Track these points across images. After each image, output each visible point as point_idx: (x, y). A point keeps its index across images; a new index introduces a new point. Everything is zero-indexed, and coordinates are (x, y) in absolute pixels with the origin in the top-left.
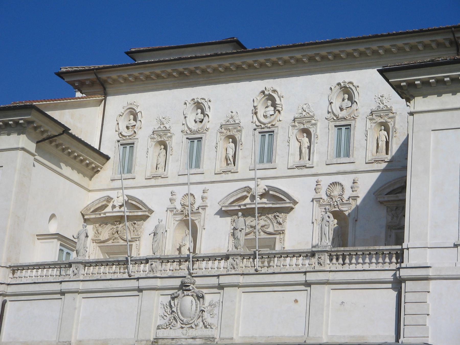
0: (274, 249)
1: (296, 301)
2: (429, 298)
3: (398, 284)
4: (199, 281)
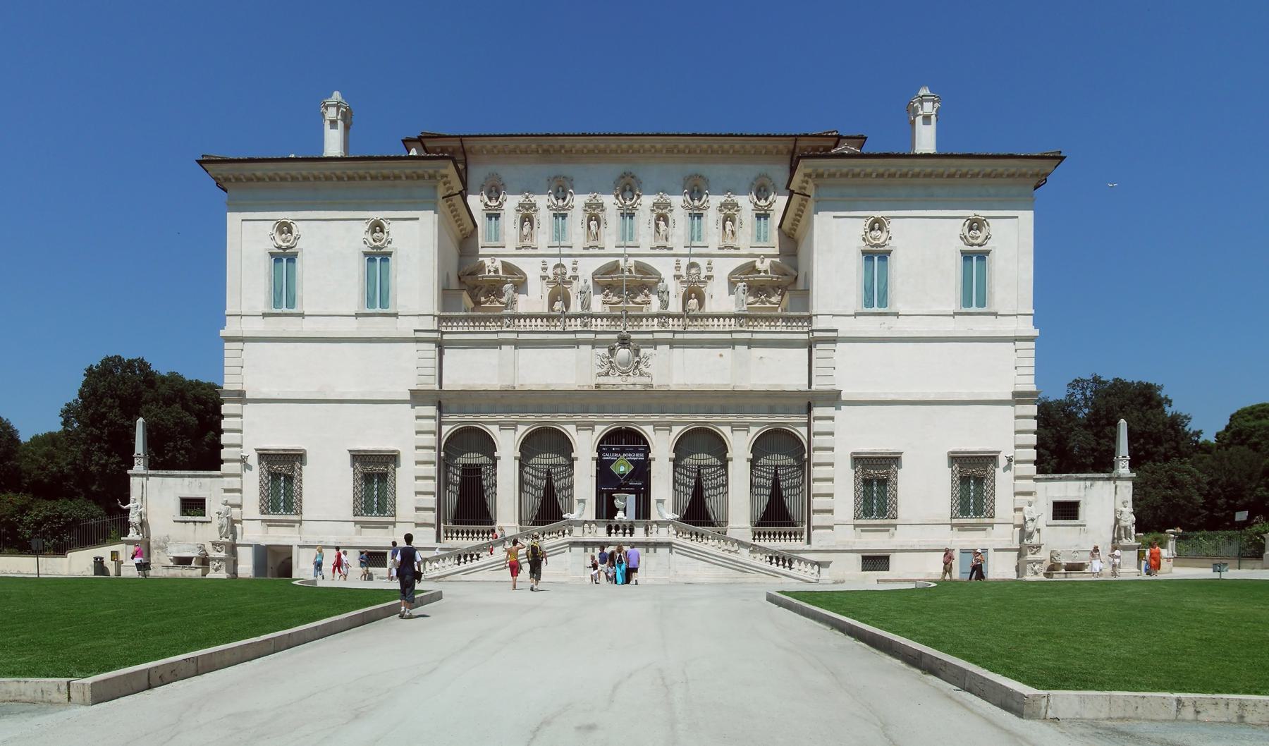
2: (835, 355)
4: (633, 337)
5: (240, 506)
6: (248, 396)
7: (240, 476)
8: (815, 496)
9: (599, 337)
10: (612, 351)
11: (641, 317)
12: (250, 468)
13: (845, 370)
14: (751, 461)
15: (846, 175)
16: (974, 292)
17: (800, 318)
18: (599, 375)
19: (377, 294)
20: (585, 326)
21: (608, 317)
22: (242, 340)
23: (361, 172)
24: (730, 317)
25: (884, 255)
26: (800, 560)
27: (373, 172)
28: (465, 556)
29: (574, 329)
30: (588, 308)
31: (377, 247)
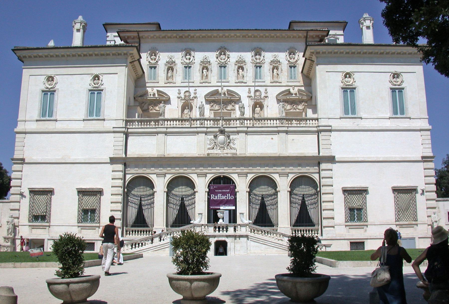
0: (231, 117)
1: (272, 139)
2: (331, 138)
5: (18, 218)
6: (26, 161)
7: (19, 202)
8: (323, 210)
9: (209, 130)
10: (216, 137)
11: (230, 120)
12: (25, 197)
13: (337, 145)
14: (290, 192)
15: (331, 53)
18: (209, 149)
19: (94, 109)
20: (202, 124)
21: (214, 120)
22: (25, 133)
23: (91, 53)
24: (276, 119)
25: (353, 90)
27: (96, 53)
29: (195, 126)
30: (203, 115)
31: (96, 87)
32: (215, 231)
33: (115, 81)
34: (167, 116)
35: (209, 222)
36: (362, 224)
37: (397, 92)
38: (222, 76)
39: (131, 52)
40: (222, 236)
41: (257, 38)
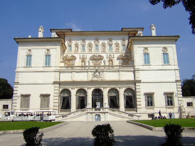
3: (134, 72)
4: (99, 70)
11: (100, 67)
16: (166, 60)
17: (132, 66)
20: (89, 68)
21: (94, 67)
26: (135, 115)
28: (64, 116)
32: (95, 111)
33: (55, 51)
34: (76, 65)
35: (93, 107)
36: (153, 107)
37: (165, 54)
38: (97, 49)
39: (62, 40)
40: (98, 113)
41: (110, 34)
